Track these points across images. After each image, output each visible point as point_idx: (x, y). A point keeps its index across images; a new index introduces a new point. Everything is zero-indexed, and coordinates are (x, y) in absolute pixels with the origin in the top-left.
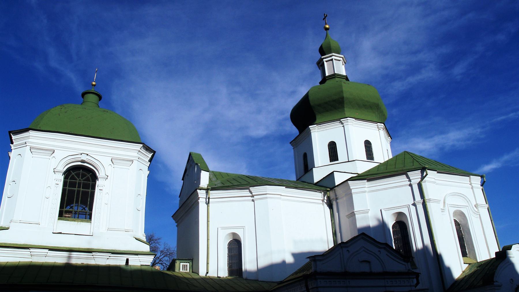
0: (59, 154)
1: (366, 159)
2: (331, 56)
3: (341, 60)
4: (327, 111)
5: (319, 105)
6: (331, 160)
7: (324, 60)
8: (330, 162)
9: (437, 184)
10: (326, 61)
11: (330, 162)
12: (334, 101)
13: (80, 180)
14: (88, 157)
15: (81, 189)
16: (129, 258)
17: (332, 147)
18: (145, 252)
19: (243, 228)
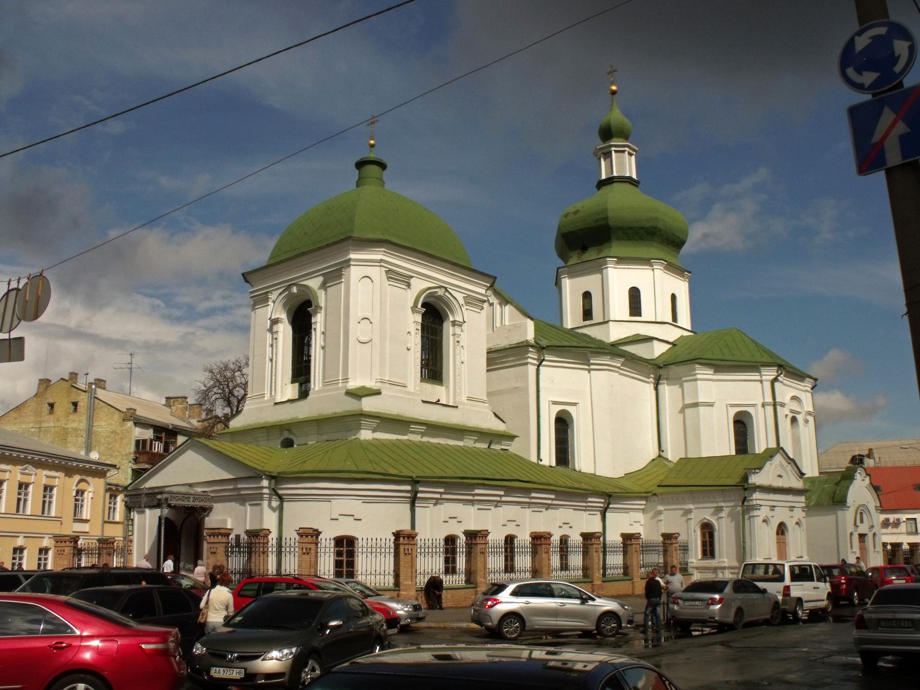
0: (418, 285)
1: (670, 321)
2: (624, 146)
3: (633, 154)
4: (630, 240)
5: (620, 228)
6: (632, 314)
7: (613, 149)
8: (631, 315)
9: (785, 385)
10: (616, 151)
11: (631, 315)
12: (643, 228)
13: (427, 322)
14: (447, 294)
15: (430, 336)
16: (493, 440)
17: (635, 295)
18: (494, 430)
19: (575, 404)
